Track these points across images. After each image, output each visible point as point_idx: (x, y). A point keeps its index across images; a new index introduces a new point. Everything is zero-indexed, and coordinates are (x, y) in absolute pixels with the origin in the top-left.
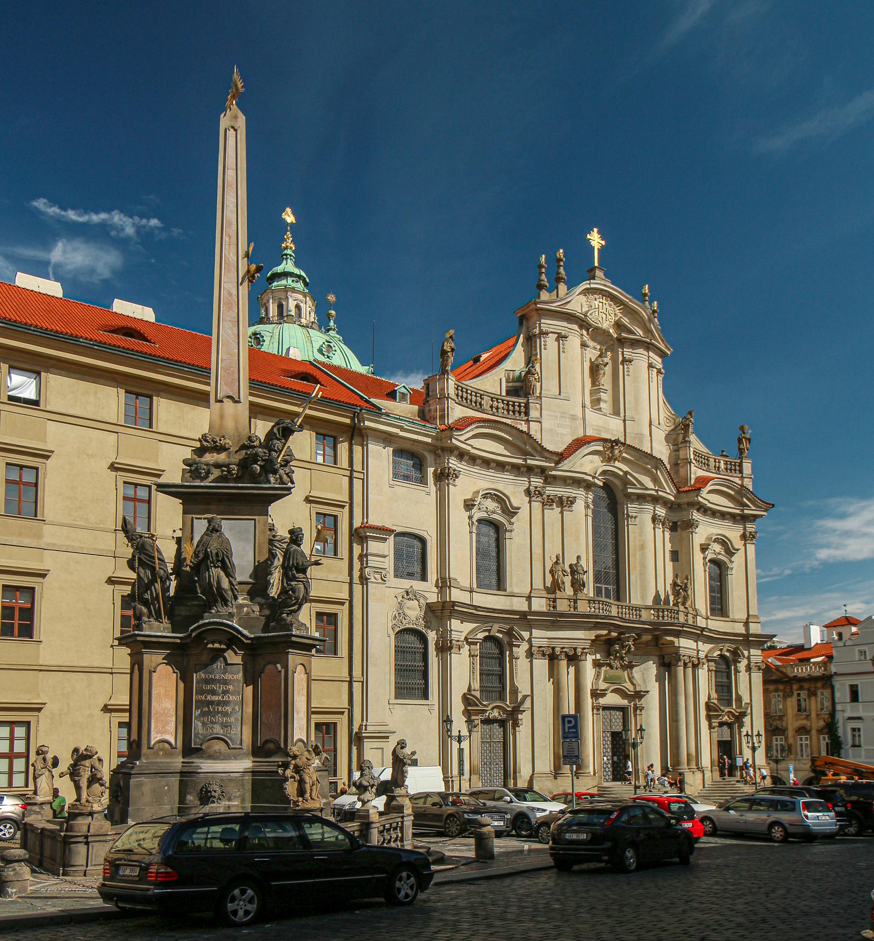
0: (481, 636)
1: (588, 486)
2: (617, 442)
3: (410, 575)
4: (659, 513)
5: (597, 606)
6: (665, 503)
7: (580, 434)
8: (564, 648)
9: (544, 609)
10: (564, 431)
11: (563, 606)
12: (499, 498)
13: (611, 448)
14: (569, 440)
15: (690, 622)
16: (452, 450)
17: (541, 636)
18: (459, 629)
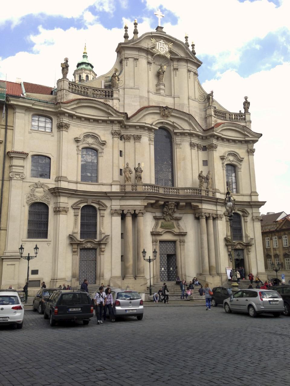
0: (82, 205)
1: (150, 129)
2: (167, 108)
3: (41, 176)
4: (193, 142)
5: (168, 190)
6: (198, 136)
7: (146, 104)
8: (129, 210)
9: (119, 191)
10: (136, 104)
11: (129, 189)
12: (95, 137)
13: (164, 111)
14: (138, 108)
15: (211, 195)
16: (63, 113)
17: (116, 204)
18: (65, 201)
